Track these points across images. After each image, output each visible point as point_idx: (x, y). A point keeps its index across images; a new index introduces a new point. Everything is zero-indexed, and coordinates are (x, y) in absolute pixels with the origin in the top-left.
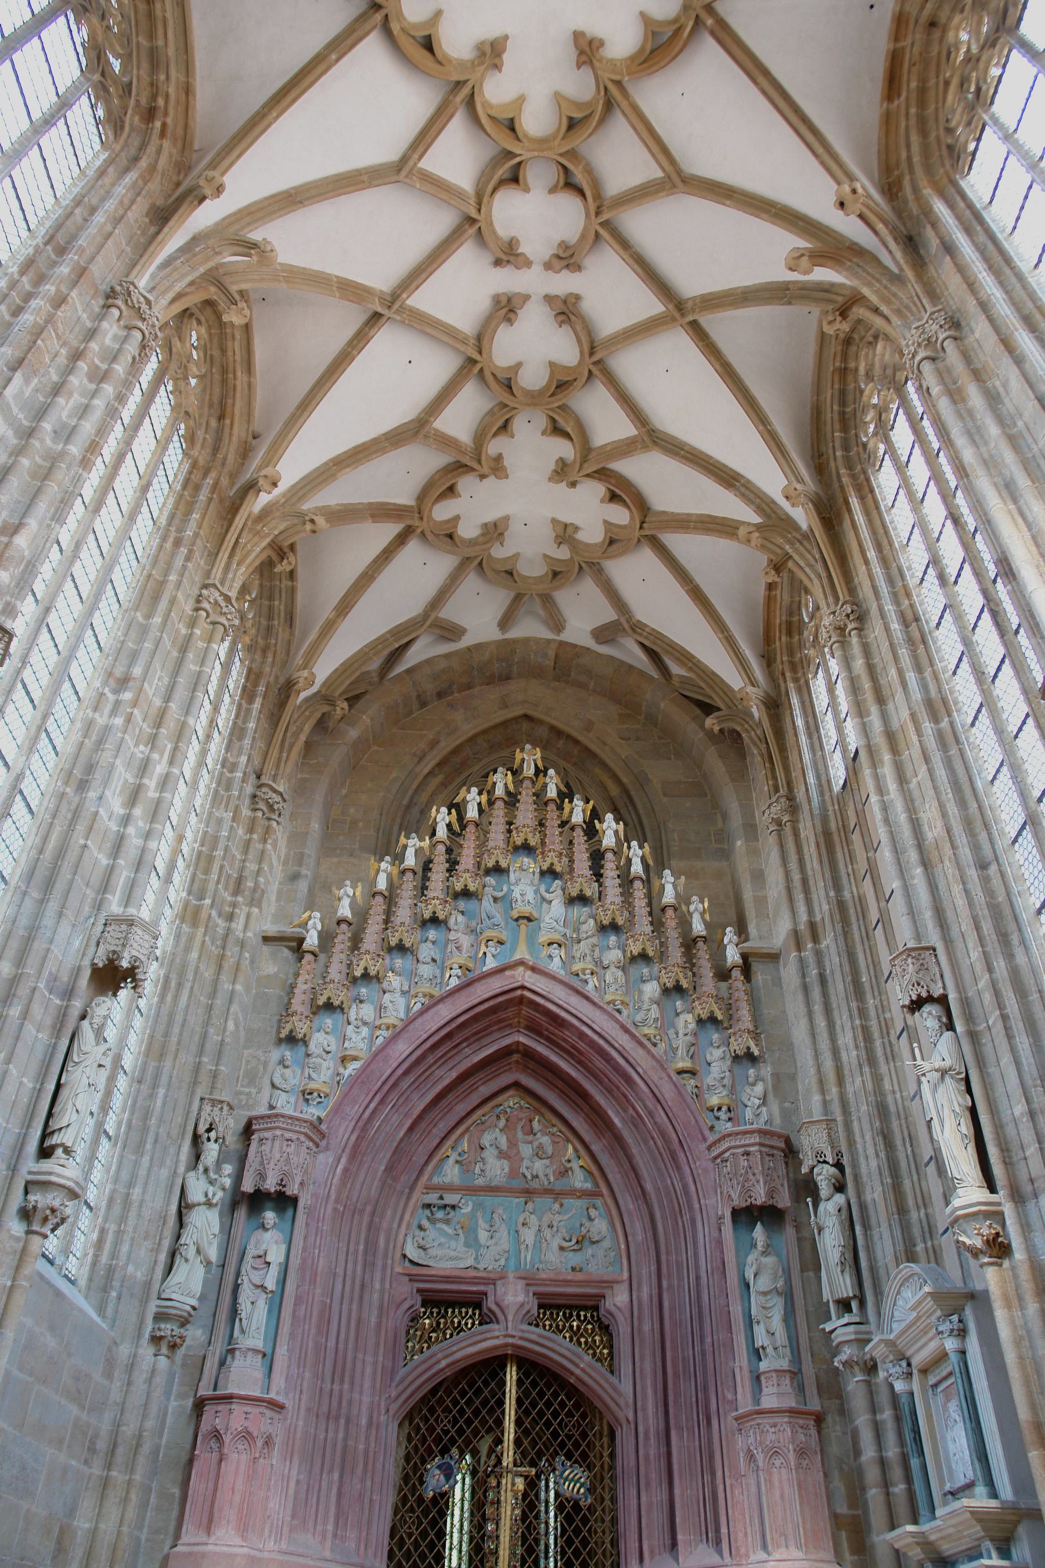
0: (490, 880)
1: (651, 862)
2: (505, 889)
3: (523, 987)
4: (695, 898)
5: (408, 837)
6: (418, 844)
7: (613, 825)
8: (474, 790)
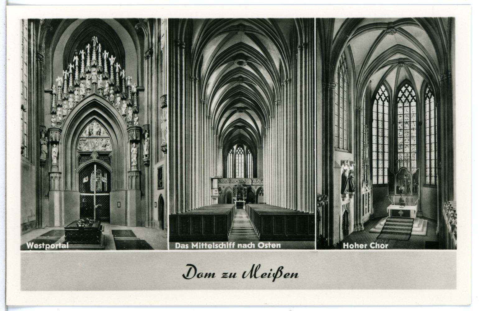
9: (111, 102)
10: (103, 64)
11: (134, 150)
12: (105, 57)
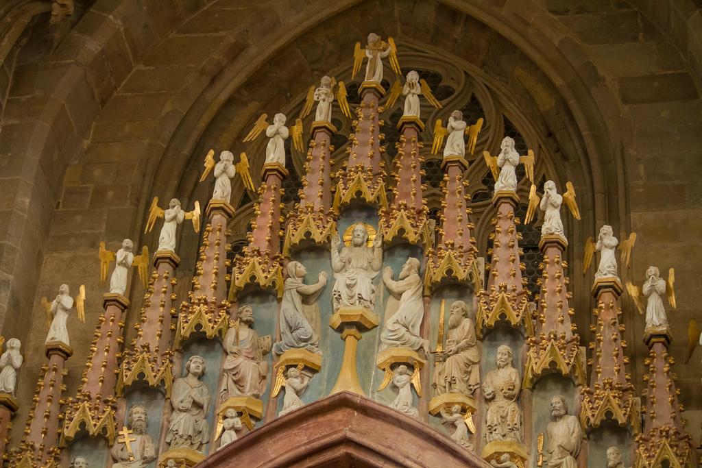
0: (294, 266)
1: (577, 215)
2: (322, 278)
3: (346, 441)
4: (652, 270)
5: (164, 205)
6: (182, 215)
7: (514, 156)
8: (280, 118)
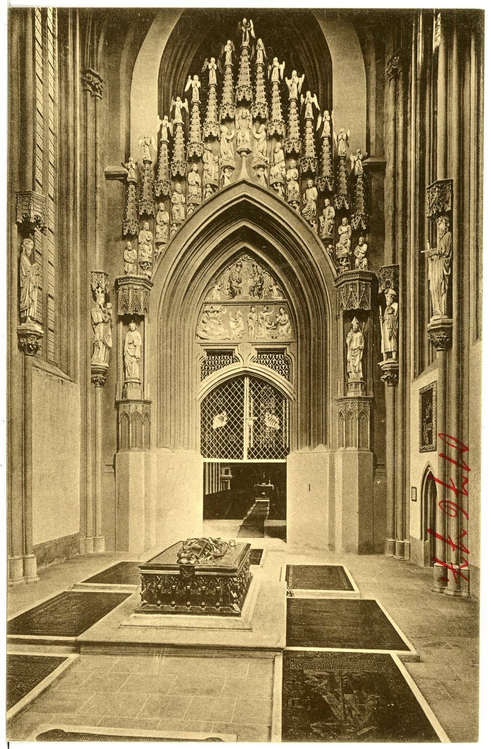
0: (224, 128)
9: (291, 202)
10: (269, 97)
11: (356, 340)
12: (275, 78)
